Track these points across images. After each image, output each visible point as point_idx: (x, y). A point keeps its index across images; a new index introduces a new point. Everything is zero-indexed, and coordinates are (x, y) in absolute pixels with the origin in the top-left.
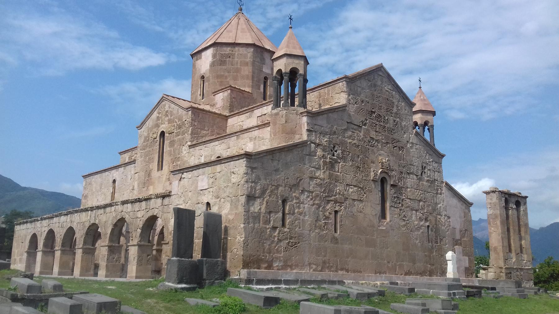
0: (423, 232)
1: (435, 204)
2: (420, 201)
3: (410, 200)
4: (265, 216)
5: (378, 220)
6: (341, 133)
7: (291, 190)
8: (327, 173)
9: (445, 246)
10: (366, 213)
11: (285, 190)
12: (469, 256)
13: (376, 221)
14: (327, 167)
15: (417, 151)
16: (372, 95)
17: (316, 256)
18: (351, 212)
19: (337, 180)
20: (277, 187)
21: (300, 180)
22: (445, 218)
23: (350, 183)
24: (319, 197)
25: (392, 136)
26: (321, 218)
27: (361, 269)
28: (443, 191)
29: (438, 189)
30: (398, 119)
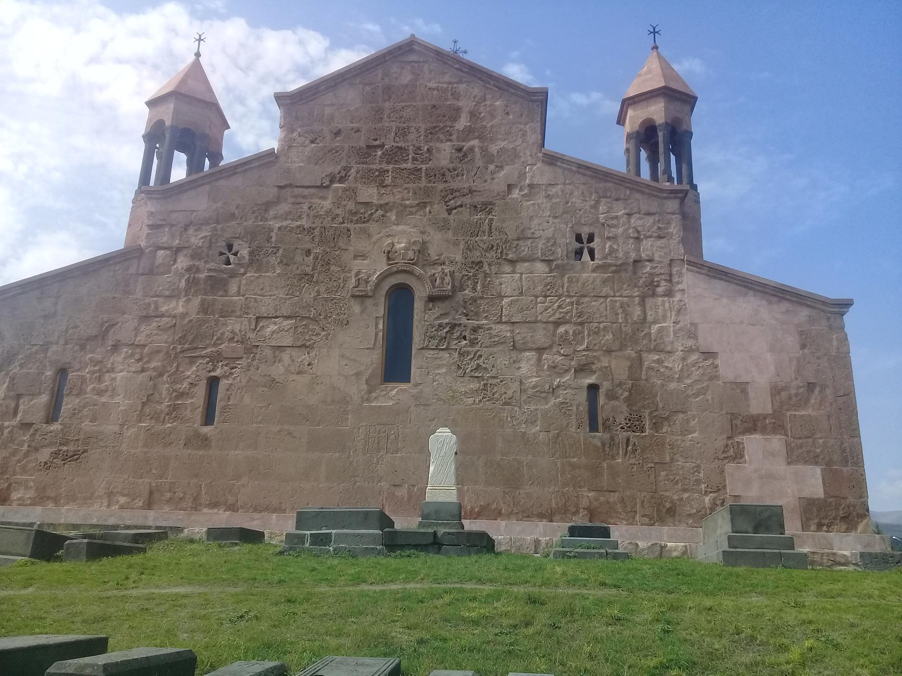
0: (563, 403)
1: (635, 323)
2: (557, 324)
3: (513, 326)
4: (4, 404)
5: (365, 387)
6: (253, 213)
7: (83, 348)
8: (197, 301)
9: (685, 435)
10: (319, 374)
11: (64, 351)
12: (829, 463)
13: (355, 390)
14: (196, 292)
15: (554, 200)
16: (373, 113)
17: (133, 477)
18: (265, 375)
19: (227, 311)
20: (45, 347)
21: (113, 325)
22: (684, 359)
23: (272, 313)
24: (164, 353)
25: (441, 186)
26: (163, 396)
27: (281, 503)
28: (680, 286)
29: (657, 281)
30: (475, 142)
